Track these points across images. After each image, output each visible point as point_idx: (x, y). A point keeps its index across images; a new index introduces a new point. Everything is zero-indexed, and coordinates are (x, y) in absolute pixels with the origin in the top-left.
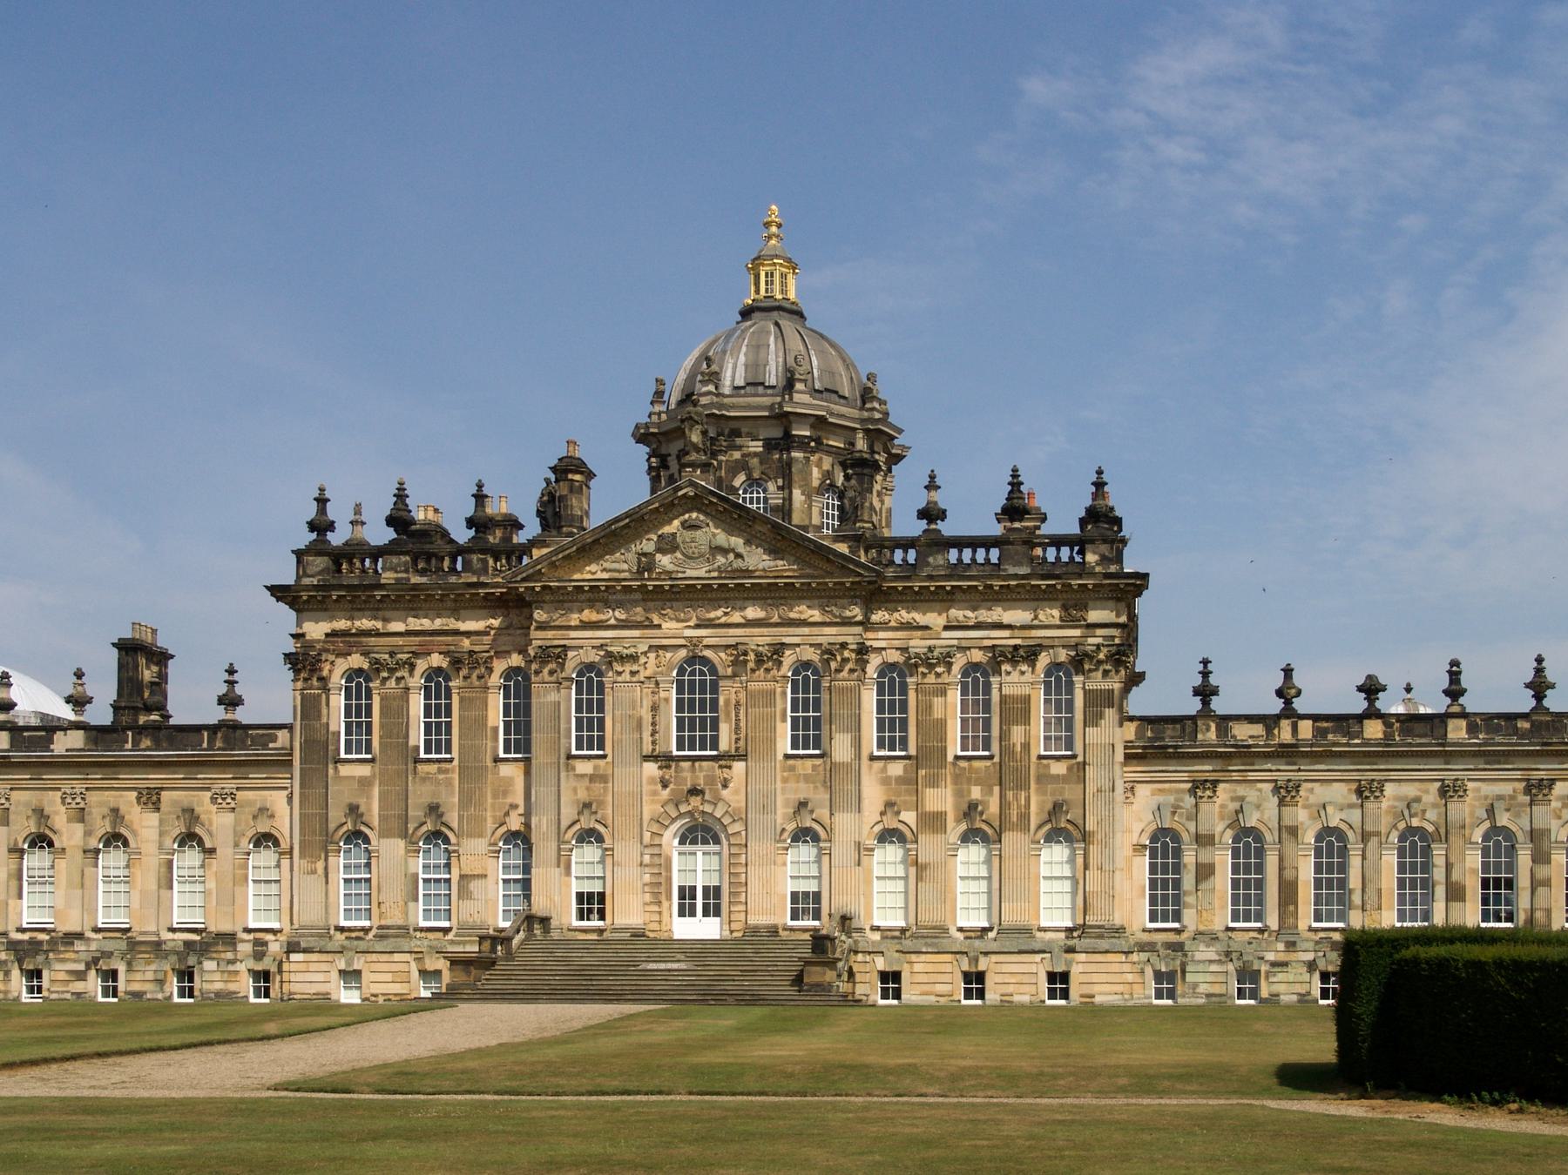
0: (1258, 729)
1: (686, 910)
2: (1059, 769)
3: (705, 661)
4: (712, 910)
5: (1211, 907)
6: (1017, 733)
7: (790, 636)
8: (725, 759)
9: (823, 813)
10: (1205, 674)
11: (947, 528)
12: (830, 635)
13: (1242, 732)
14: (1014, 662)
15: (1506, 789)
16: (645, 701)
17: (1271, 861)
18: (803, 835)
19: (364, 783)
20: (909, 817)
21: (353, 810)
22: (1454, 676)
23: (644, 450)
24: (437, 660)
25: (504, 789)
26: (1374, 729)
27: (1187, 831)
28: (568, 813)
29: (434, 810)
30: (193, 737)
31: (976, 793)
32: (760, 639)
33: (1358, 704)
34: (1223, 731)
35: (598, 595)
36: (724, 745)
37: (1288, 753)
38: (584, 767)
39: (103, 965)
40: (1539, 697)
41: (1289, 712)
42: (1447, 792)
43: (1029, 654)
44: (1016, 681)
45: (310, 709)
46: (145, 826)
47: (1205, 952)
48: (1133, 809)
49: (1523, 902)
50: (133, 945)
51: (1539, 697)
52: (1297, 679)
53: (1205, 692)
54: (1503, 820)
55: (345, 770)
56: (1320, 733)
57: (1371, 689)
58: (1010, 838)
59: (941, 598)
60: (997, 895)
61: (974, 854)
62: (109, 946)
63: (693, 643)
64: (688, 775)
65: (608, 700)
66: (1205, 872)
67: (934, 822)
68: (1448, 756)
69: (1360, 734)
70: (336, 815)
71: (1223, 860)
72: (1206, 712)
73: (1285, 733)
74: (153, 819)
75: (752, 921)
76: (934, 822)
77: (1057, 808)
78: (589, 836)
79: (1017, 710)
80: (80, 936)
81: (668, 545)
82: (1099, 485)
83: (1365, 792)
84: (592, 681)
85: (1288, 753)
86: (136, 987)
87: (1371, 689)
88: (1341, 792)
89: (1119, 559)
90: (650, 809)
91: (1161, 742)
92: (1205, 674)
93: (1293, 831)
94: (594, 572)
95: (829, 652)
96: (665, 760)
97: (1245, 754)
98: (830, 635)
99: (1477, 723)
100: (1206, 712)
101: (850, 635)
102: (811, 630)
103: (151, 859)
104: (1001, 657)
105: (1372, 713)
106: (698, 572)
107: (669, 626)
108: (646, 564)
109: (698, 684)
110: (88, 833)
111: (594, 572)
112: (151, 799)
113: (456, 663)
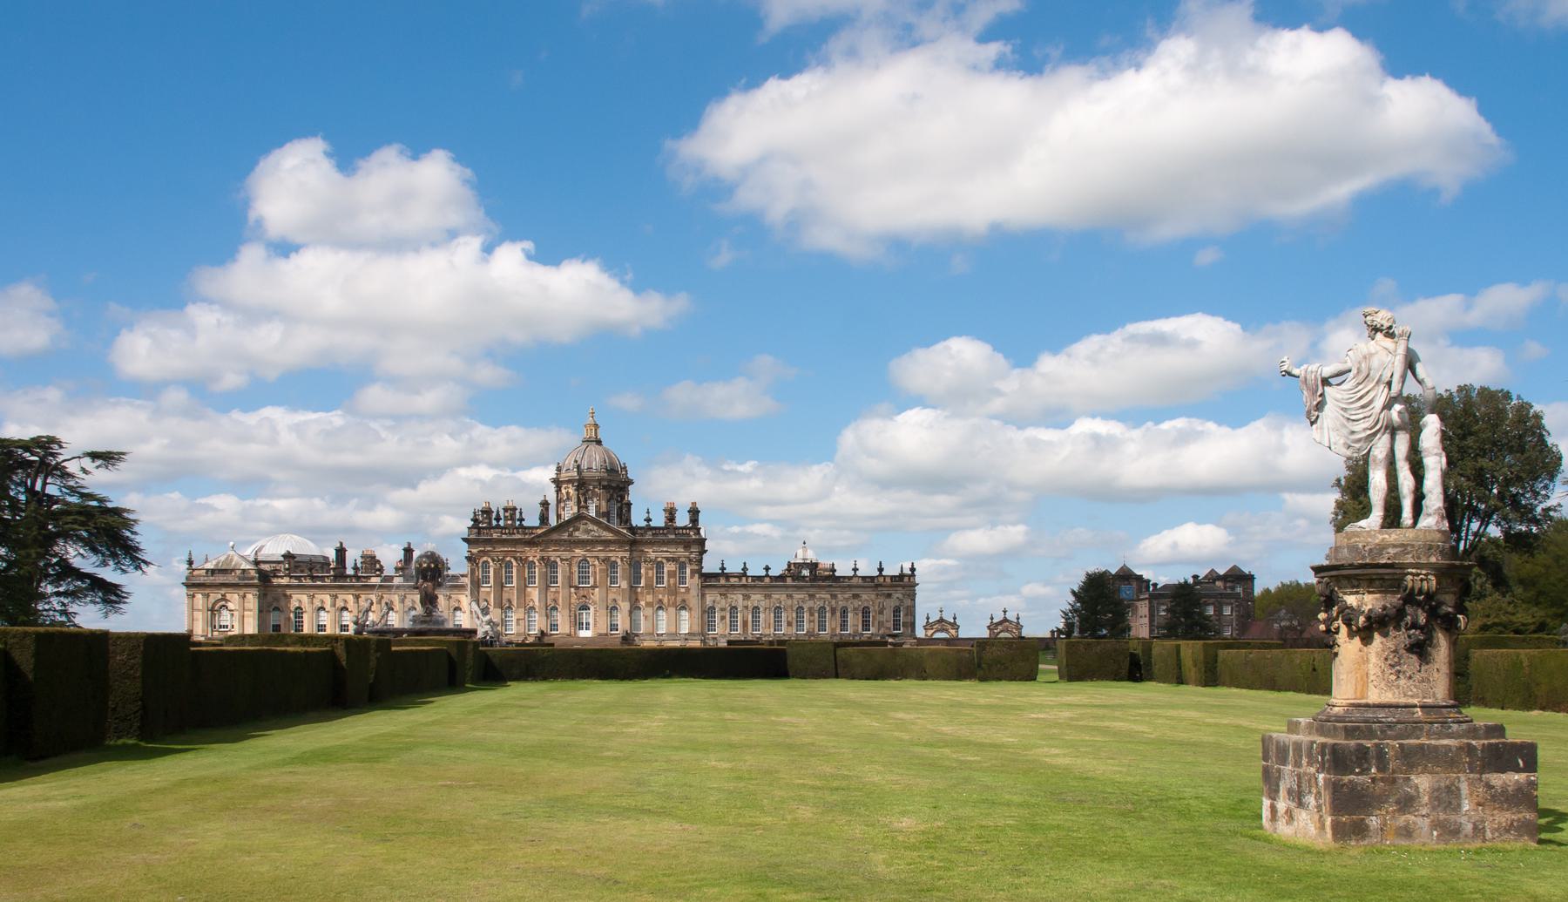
8: (594, 587)
11: (652, 524)
13: (733, 581)
26: (767, 580)
32: (602, 555)
33: (763, 573)
37: (744, 586)
41: (744, 574)
43: (673, 560)
45: (473, 571)
53: (723, 568)
57: (767, 569)
67: (649, 604)
68: (787, 587)
73: (744, 581)
76: (649, 604)
87: (767, 569)
96: (577, 588)
97: (733, 586)
98: (621, 554)
101: (627, 554)
104: (668, 559)
111: (555, 536)
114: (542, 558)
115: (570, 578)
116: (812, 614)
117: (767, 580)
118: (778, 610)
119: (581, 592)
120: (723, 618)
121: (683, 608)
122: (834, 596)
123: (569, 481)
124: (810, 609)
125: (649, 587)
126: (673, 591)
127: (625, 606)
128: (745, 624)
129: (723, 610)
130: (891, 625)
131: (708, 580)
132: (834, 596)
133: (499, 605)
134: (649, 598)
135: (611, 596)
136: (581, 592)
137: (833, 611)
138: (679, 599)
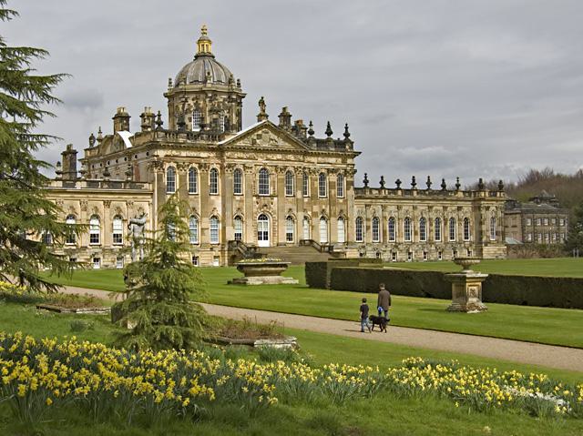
0: (377, 192)
1: (260, 239)
2: (341, 201)
3: (265, 169)
4: (266, 238)
5: (368, 237)
6: (333, 191)
7: (287, 164)
10: (366, 177)
12: (297, 164)
14: (332, 172)
15: (424, 208)
16: (249, 180)
17: (380, 225)
20: (310, 213)
22: (414, 180)
23: (167, 100)
25: (213, 203)
26: (400, 192)
27: (364, 217)
28: (235, 211)
30: (119, 185)
31: (324, 207)
32: (280, 164)
34: (371, 192)
36: (271, 192)
38: (238, 198)
39: (96, 256)
40: (429, 186)
41: (382, 188)
42: (414, 208)
43: (333, 171)
44: (333, 178)
46: (106, 213)
47: (369, 248)
48: (355, 209)
49: (427, 235)
50: (104, 250)
51: (429, 186)
52: (384, 179)
54: (424, 216)
56: (389, 193)
57: (398, 183)
58: (332, 219)
59: (317, 155)
60: (329, 234)
61: (323, 222)
62: (97, 250)
63: (265, 164)
64: (263, 201)
65: (243, 179)
66: (368, 228)
67: (315, 214)
68: (414, 200)
71: (371, 224)
72: (366, 187)
74: (108, 210)
76: (315, 214)
77: (341, 211)
78: (238, 218)
79: (331, 185)
80: (86, 247)
81: (259, 137)
82: (347, 128)
83: (399, 208)
84: (238, 174)
85: (385, 198)
86: (105, 263)
87: (398, 183)
88: (393, 208)
89: (352, 147)
90: (255, 210)
91: (361, 193)
92: (366, 177)
93: (385, 217)
96: (258, 197)
99: (420, 192)
100: (366, 187)
102: (292, 162)
103: (108, 223)
105: (398, 189)
107: (260, 159)
109: (264, 173)
110: (88, 215)
112: (107, 204)
113: (178, 166)
114: (229, 166)
115: (253, 187)
116: (431, 225)
117: (400, 192)
118: (408, 221)
120: (368, 228)
121: (341, 218)
122: (445, 208)
124: (430, 219)
125: (313, 197)
126: (331, 202)
127: (301, 215)
128: (384, 232)
129: (368, 220)
131: (361, 193)
132: (445, 208)
134: (316, 208)
136: (263, 201)
138: (338, 210)
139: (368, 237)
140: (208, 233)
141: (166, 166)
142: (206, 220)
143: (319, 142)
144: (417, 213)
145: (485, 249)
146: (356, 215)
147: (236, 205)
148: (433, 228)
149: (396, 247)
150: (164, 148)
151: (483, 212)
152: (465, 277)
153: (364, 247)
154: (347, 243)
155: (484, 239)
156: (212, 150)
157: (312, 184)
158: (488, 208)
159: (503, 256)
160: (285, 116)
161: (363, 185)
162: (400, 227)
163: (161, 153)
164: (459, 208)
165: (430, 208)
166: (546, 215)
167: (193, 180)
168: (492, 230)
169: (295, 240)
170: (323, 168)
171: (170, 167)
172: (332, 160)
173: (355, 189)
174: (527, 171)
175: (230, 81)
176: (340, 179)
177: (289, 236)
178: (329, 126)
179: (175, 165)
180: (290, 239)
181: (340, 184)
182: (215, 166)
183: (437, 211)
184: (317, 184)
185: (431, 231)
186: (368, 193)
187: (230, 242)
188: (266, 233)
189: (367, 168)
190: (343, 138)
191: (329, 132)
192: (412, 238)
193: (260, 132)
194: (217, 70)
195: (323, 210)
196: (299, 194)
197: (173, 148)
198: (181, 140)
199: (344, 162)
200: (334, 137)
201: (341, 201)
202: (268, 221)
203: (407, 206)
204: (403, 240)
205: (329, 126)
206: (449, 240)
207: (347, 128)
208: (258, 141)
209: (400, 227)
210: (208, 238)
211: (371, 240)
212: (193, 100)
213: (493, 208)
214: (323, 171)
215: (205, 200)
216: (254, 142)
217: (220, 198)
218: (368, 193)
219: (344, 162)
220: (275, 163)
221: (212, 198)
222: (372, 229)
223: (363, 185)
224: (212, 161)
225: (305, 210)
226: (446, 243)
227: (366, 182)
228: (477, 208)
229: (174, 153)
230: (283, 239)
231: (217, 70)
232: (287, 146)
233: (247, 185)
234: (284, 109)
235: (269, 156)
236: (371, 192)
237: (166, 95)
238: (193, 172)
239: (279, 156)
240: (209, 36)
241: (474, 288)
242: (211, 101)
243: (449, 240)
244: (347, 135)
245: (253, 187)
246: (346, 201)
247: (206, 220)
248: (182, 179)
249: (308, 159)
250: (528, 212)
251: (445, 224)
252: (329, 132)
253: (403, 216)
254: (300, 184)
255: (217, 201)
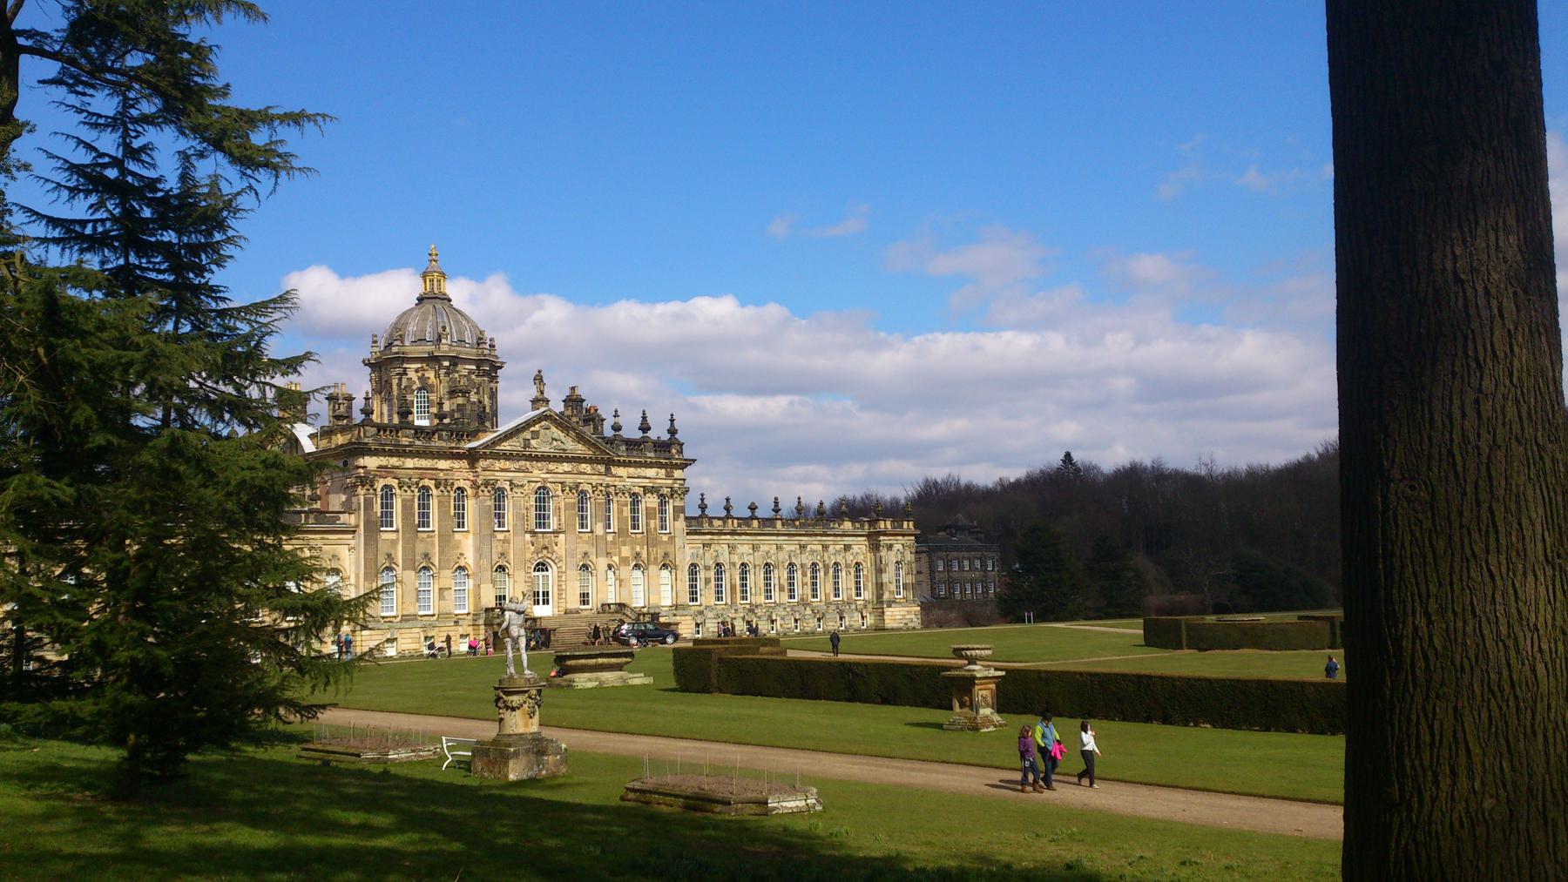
2: (665, 538)
3: (544, 488)
4: (546, 602)
5: (707, 597)
6: (652, 525)
9: (593, 558)
12: (595, 480)
17: (726, 577)
18: (585, 567)
19: (394, 543)
20: (616, 559)
21: (389, 556)
22: (776, 503)
24: (426, 482)
25: (458, 545)
26: (755, 523)
27: (701, 563)
28: (495, 558)
29: (426, 556)
32: (569, 479)
33: (748, 514)
34: (711, 524)
35: (508, 456)
38: (500, 536)
41: (729, 516)
42: (779, 548)
47: (710, 615)
49: (798, 591)
55: (384, 536)
57: (753, 508)
58: (652, 567)
61: (638, 573)
63: (545, 480)
66: (707, 581)
67: (624, 561)
69: (749, 526)
70: (382, 559)
71: (712, 574)
75: (570, 606)
76: (624, 561)
78: (502, 568)
79: (650, 514)
81: (536, 435)
82: (672, 421)
83: (755, 548)
84: (499, 495)
85: (733, 533)
87: (753, 508)
88: (746, 549)
90: (528, 556)
94: (506, 446)
95: (595, 488)
96: (533, 533)
98: (595, 480)
102: (589, 476)
106: (546, 449)
108: (527, 444)
111: (506, 446)
115: (525, 518)
116: (804, 574)
117: (755, 523)
119: (541, 541)
120: (707, 581)
122: (825, 547)
123: (433, 360)
125: (621, 533)
126: (650, 540)
127: (602, 563)
128: (733, 588)
129: (707, 568)
130: (893, 587)
132: (825, 547)
133: (410, 564)
135: (583, 548)
136: (541, 541)
137: (826, 567)
138: (661, 552)
139: (707, 597)
140: (450, 595)
141: (380, 484)
142: (448, 573)
143: (631, 444)
144: (783, 556)
145: (888, 612)
146: (688, 560)
147: (497, 548)
148: (808, 579)
149: (751, 611)
150: (376, 453)
151: (883, 553)
152: (975, 678)
153: (701, 613)
154: (676, 607)
155: (886, 596)
156: (458, 457)
157: (620, 512)
158: (890, 547)
159: (916, 623)
160: (573, 401)
161: (698, 513)
162: (756, 579)
163: (371, 462)
164: (847, 548)
165: (803, 547)
166: (966, 554)
167: (424, 506)
168: (898, 581)
169: (594, 603)
170: (636, 485)
171: (386, 486)
172: (651, 472)
173: (687, 518)
174: (921, 480)
175: (480, 341)
176: (663, 504)
177: (584, 598)
178: (644, 418)
179: (394, 483)
180: (584, 602)
181: (663, 511)
182: (461, 484)
183: (813, 552)
184: (627, 511)
185: (804, 584)
186: (706, 526)
187: (487, 610)
188: (546, 594)
189: (708, 482)
190: (665, 437)
191: (645, 428)
192: (776, 596)
193: (537, 428)
194: (457, 322)
195: (638, 554)
196: (599, 529)
197: (391, 454)
198: (405, 441)
199: (669, 476)
200: (652, 435)
201: (665, 538)
202: (549, 573)
203: (768, 545)
204: (762, 599)
205: (644, 418)
206: (833, 598)
207: (672, 421)
208: (533, 442)
209: (756, 579)
210: (450, 605)
211: (713, 601)
212: (417, 371)
213: (898, 546)
214: (636, 490)
215: (446, 539)
216: (527, 444)
217: (471, 536)
218: (706, 526)
219: (669, 476)
220: (561, 478)
221: (457, 536)
222: (713, 583)
223: (698, 513)
224: (457, 475)
225: (608, 554)
226: (828, 604)
227: (703, 507)
228: (875, 547)
229: (394, 461)
230: (574, 603)
231: (457, 322)
232: (580, 449)
233: (517, 515)
234: (573, 389)
235: (552, 466)
236: (711, 524)
237: (367, 363)
238: (425, 492)
239: (566, 467)
240: (442, 265)
241: (983, 693)
242: (447, 374)
243: (833, 598)
244: (673, 432)
245: (525, 518)
246: (672, 538)
247: (448, 573)
248: (407, 506)
249: (614, 470)
250: (939, 549)
251: (826, 573)
252: (645, 428)
253: (760, 562)
254: (601, 513)
255: (467, 544)
